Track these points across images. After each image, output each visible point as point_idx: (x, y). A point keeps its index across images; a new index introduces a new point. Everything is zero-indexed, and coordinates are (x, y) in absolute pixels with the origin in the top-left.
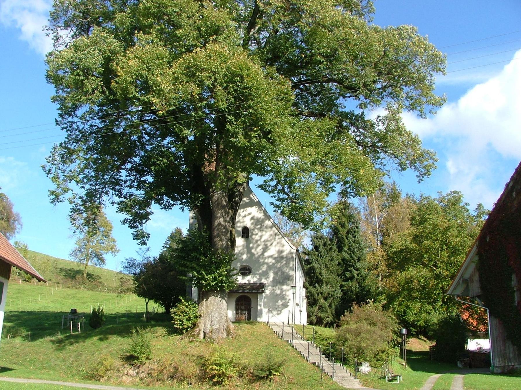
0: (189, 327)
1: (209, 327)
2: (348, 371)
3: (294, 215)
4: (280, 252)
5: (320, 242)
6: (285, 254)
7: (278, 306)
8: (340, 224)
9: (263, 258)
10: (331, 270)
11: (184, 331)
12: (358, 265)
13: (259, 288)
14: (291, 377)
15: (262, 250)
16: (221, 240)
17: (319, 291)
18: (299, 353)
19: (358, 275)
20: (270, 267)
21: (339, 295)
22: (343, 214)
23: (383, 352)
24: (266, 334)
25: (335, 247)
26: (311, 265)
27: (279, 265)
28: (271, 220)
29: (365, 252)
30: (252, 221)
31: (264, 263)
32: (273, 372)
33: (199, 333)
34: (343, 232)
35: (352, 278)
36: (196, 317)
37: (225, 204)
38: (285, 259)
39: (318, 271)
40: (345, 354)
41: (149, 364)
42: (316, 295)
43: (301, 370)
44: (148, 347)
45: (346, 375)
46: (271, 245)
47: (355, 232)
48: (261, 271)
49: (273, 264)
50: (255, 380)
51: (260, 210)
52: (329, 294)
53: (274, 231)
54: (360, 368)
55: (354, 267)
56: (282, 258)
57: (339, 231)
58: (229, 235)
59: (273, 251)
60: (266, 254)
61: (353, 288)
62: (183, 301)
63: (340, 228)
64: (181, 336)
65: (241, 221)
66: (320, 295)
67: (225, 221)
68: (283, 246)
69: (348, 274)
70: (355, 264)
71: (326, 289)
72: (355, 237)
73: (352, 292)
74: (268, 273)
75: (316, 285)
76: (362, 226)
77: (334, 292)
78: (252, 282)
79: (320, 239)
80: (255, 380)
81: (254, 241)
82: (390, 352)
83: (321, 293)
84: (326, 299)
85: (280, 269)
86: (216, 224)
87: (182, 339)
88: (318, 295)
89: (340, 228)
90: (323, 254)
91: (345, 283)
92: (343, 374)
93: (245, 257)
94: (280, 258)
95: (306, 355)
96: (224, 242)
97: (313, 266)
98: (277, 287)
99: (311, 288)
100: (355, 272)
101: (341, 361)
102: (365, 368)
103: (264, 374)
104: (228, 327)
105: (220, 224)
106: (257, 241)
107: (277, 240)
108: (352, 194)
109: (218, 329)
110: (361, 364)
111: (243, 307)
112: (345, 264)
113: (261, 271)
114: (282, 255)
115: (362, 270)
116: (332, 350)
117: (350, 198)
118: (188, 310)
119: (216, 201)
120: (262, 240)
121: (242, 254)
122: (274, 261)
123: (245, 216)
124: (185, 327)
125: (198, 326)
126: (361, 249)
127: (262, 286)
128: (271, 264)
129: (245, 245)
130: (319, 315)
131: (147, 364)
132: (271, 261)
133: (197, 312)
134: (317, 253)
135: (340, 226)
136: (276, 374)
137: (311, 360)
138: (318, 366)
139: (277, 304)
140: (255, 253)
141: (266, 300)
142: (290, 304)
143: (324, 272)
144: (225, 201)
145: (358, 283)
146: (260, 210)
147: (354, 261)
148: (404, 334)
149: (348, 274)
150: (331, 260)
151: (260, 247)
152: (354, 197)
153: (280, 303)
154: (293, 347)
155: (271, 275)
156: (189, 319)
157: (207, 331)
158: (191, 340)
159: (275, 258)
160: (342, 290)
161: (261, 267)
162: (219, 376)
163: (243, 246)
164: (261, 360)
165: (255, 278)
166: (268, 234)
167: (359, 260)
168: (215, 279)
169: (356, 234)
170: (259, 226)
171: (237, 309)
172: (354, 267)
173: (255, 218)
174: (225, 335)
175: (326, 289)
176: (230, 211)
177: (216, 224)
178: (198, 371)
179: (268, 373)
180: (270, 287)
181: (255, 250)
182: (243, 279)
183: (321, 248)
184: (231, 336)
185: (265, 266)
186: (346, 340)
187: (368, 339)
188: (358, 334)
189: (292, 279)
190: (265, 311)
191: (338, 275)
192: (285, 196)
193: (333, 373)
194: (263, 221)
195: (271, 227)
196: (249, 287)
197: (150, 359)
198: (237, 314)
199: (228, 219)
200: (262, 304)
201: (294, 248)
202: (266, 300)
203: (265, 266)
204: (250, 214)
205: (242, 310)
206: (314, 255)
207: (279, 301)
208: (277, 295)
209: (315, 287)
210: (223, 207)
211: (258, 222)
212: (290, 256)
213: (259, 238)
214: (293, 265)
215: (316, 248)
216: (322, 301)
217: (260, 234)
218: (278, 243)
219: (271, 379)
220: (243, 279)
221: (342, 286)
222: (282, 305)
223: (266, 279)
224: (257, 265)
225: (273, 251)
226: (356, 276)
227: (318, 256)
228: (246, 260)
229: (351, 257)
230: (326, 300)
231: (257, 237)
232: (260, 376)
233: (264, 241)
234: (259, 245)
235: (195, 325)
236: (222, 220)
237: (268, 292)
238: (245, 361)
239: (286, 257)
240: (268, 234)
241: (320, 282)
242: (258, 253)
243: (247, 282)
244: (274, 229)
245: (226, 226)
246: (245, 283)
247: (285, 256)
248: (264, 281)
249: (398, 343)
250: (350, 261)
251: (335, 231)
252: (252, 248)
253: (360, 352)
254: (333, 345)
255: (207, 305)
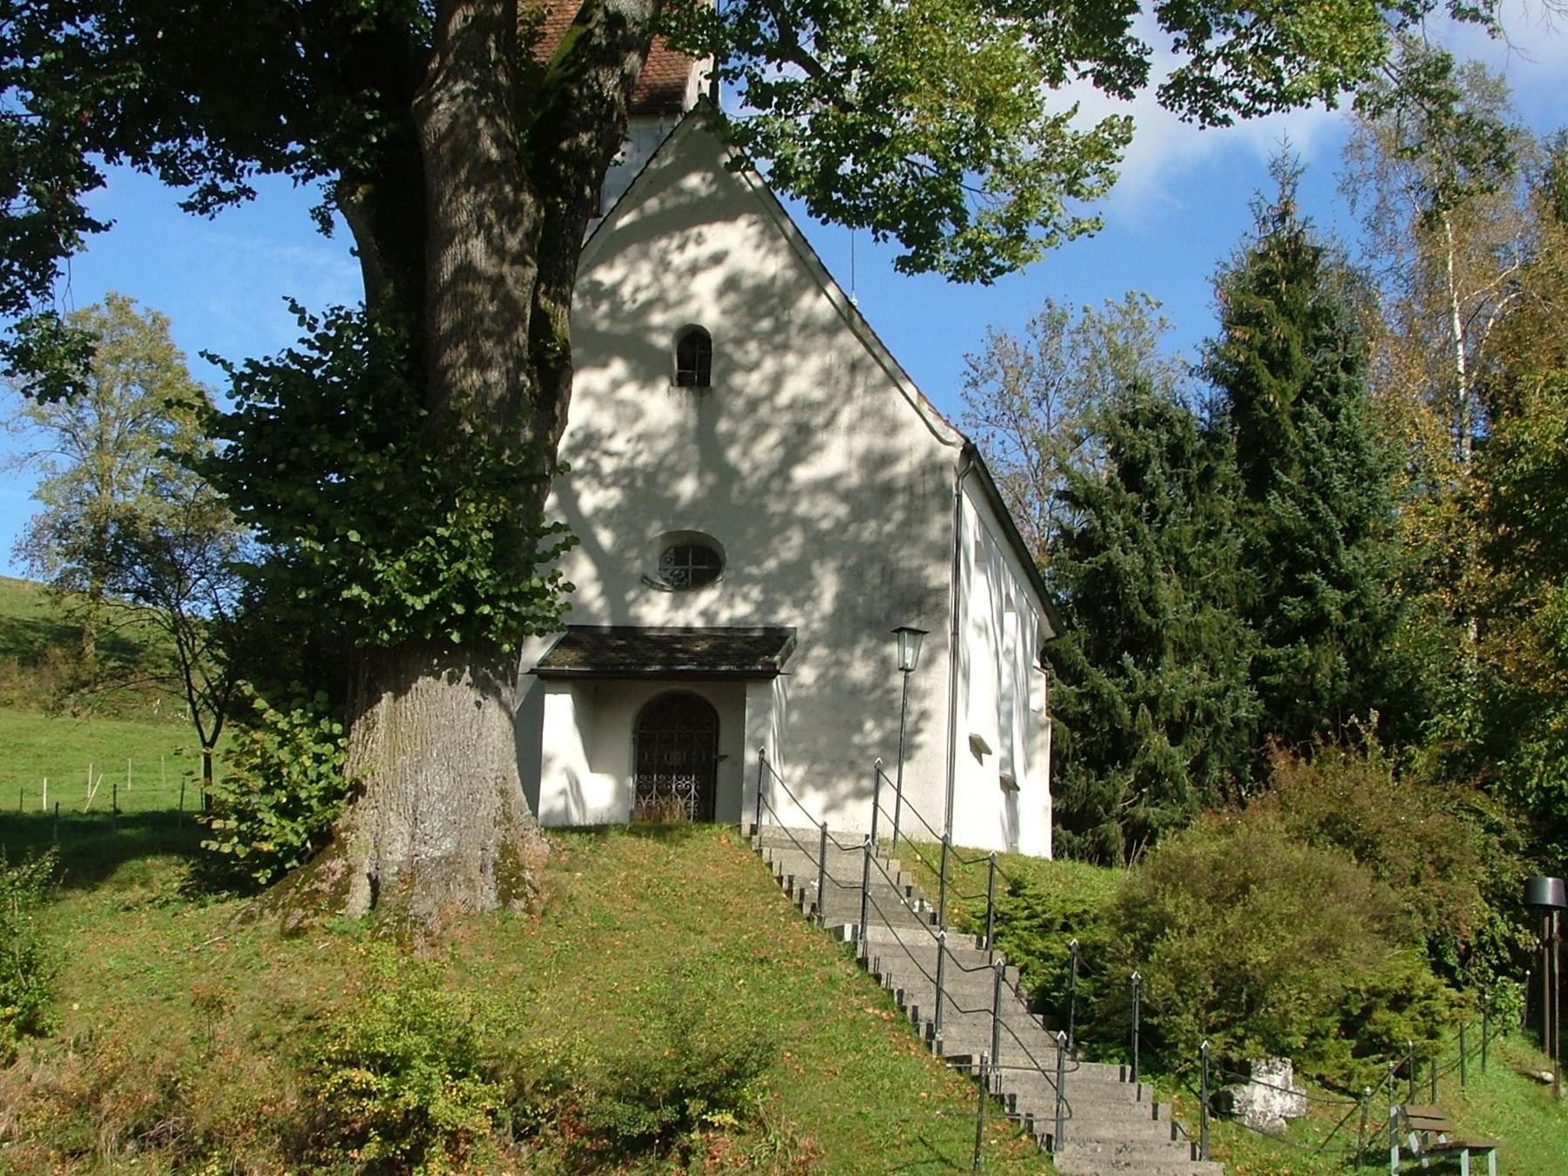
0: (290, 851)
1: (398, 853)
2: (1165, 1109)
3: (850, 186)
4: (876, 462)
5: (1149, 443)
6: (902, 468)
7: (862, 749)
8: (1263, 352)
9: (782, 494)
10: (1204, 587)
11: (262, 876)
12: (1349, 558)
13: (753, 655)
14: (803, 1142)
15: (779, 453)
16: (480, 362)
17: (1139, 692)
18: (895, 1001)
19: (1347, 610)
20: (820, 544)
21: (1242, 713)
22: (1279, 302)
23: (1399, 1002)
24: (730, 895)
25: (1227, 469)
26: (1101, 559)
27: (869, 531)
28: (831, 290)
29: (1384, 491)
30: (731, 298)
31: (788, 520)
32: (695, 1107)
33: (343, 888)
34: (1277, 394)
35: (1314, 627)
36: (331, 795)
37: (494, 153)
38: (901, 499)
39: (1133, 588)
40: (1147, 1010)
41: (36, 1059)
42: (1126, 712)
43: (872, 1099)
44: (29, 966)
45: (1148, 1132)
46: (829, 423)
47: (1334, 389)
48: (771, 564)
49: (841, 526)
50: (601, 1155)
51: (774, 238)
52: (1192, 706)
53: (842, 351)
54: (1240, 1093)
55: (1325, 567)
56: (888, 491)
57: (1259, 391)
58: (522, 336)
59: (835, 457)
60: (803, 474)
61: (1322, 678)
62: (260, 703)
63: (1266, 377)
64: (247, 902)
65: (673, 295)
66: (1144, 709)
67: (496, 249)
68: (894, 428)
69: (1294, 608)
70: (1333, 552)
71: (1178, 680)
72: (1333, 416)
73: (1315, 696)
74: (810, 577)
75: (1128, 659)
76: (1380, 361)
77: (1220, 695)
78: (724, 617)
79: (1150, 425)
80: (601, 1155)
81: (739, 404)
82: (1439, 1006)
83: (1152, 703)
84: (1176, 733)
85: (876, 554)
86: (447, 272)
87: (249, 918)
88: (1134, 712)
89: (1266, 377)
90: (1163, 500)
91: (1281, 651)
92: (1127, 1131)
93: (687, 487)
94: (874, 490)
95: (927, 1012)
96: (494, 375)
97: (1109, 564)
98: (858, 652)
99: (1099, 677)
100: (1332, 598)
101: (1128, 1058)
102: (1271, 1095)
103: (648, 1122)
104: (506, 850)
105: (466, 271)
106: (753, 405)
107: (862, 399)
108: (1240, 96)
109: (447, 860)
110: (1243, 1072)
111: (676, 758)
112: (1285, 558)
113: (771, 564)
114: (885, 475)
115: (1370, 583)
116: (1082, 985)
117: (1226, 121)
118: (284, 754)
119: (442, 139)
120: (783, 398)
121: (677, 474)
122: (842, 510)
123: (694, 269)
124: (267, 847)
125: (342, 846)
126: (1364, 476)
127: (777, 639)
128: (826, 525)
129: (692, 422)
130: (1141, 812)
131: (24, 1063)
132: (829, 511)
133: (338, 770)
134: (1132, 497)
135: (1260, 362)
136: (716, 1119)
137: (953, 1039)
138: (981, 1081)
139: (857, 739)
140: (745, 467)
141: (795, 717)
142: (932, 738)
143: (1168, 592)
144: (498, 139)
145: (1350, 653)
146: (774, 238)
147: (1326, 531)
148: (1548, 910)
149: (1294, 608)
150: (1210, 535)
151: (772, 438)
152: (1246, 114)
153: (872, 731)
154: (863, 963)
155: (828, 587)
156: (289, 810)
157: (389, 875)
158: (292, 923)
159: (846, 496)
160: (1264, 690)
161: (776, 541)
162: (390, 1132)
163: (681, 429)
164: (650, 1045)
165: (738, 600)
166: (814, 364)
167: (1354, 531)
168: (426, 576)
169: (1342, 398)
170: (766, 324)
171: (642, 768)
172: (1325, 567)
173: (748, 283)
174: (488, 898)
175: (1178, 680)
176: (528, 199)
177: (447, 272)
178: (292, 1101)
179: (669, 1114)
180: (819, 651)
181: (745, 453)
182: (677, 605)
183: (1155, 472)
184: (519, 904)
185: (796, 538)
186: (1162, 923)
187: (1289, 921)
188: (1231, 890)
189: (939, 608)
190: (785, 774)
191: (1246, 612)
192: (794, 72)
193: (1059, 1120)
194: (787, 297)
195: (831, 330)
196: (701, 647)
197: (41, 1034)
198: (641, 791)
199: (513, 243)
200: (766, 731)
201: (952, 436)
202: (795, 717)
203: (796, 538)
204: (717, 259)
205: (667, 771)
206: (1119, 507)
207: (869, 725)
208: (855, 691)
209: (1122, 671)
210: (485, 173)
211: (758, 302)
212: (930, 484)
213: (764, 390)
214: (946, 529)
215: (1131, 472)
216: (1158, 741)
217: (769, 365)
218: (864, 414)
219: (686, 1152)
220: (677, 605)
221: (1260, 667)
222: (884, 743)
223: (798, 604)
224: (752, 531)
225: (835, 457)
226: (1335, 614)
227: (1137, 512)
228: (695, 503)
229: (1314, 516)
230: (1175, 740)
231: (753, 383)
232: (624, 1131)
233: (791, 406)
234: (762, 428)
235: (324, 838)
236: (477, 248)
237: (807, 674)
238: (545, 1045)
239: (909, 488)
240: (814, 364)
241: (1147, 645)
242: (755, 468)
243: (699, 623)
244: (846, 339)
245: (502, 278)
246: (688, 629)
247: (901, 483)
248: (787, 616)
249: (1520, 957)
250: (1306, 538)
251: (1241, 388)
252: (732, 438)
253: (1239, 999)
254: (1089, 961)
255: (393, 721)
